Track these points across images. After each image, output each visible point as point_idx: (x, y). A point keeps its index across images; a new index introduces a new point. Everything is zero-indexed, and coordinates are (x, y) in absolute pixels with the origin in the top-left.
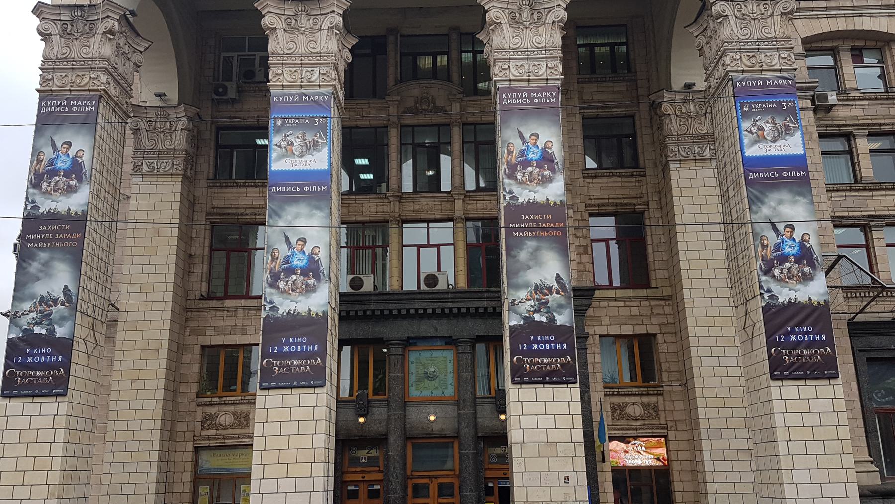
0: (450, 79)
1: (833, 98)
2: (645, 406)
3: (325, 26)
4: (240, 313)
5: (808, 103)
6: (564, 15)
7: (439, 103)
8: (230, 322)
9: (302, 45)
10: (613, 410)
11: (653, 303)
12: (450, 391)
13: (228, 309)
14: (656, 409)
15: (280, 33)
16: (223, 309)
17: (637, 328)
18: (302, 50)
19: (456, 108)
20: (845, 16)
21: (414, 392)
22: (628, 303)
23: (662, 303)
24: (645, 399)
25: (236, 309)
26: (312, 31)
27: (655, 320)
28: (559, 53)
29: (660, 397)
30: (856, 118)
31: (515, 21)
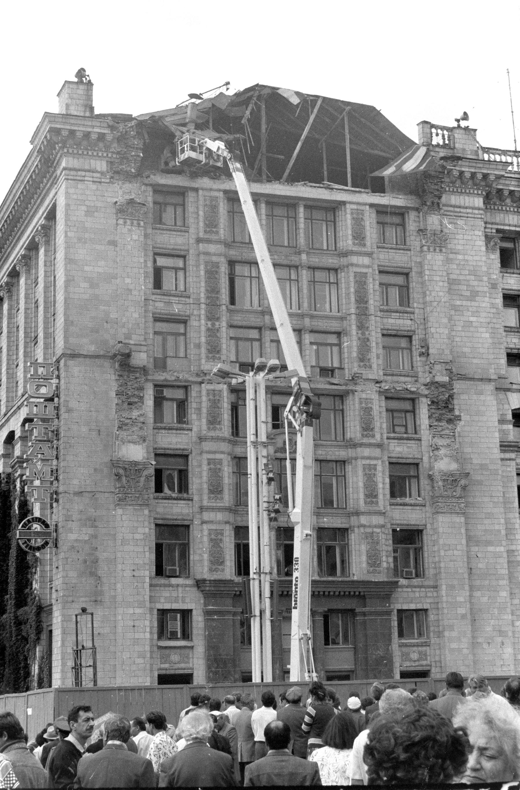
2: (420, 653)
4: (180, 589)
8: (174, 594)
10: (403, 655)
11: (427, 590)
13: (170, 585)
14: (426, 655)
16: (170, 585)
17: (418, 605)
22: (414, 589)
23: (432, 589)
24: (420, 649)
25: (178, 586)
27: (429, 600)
29: (428, 648)
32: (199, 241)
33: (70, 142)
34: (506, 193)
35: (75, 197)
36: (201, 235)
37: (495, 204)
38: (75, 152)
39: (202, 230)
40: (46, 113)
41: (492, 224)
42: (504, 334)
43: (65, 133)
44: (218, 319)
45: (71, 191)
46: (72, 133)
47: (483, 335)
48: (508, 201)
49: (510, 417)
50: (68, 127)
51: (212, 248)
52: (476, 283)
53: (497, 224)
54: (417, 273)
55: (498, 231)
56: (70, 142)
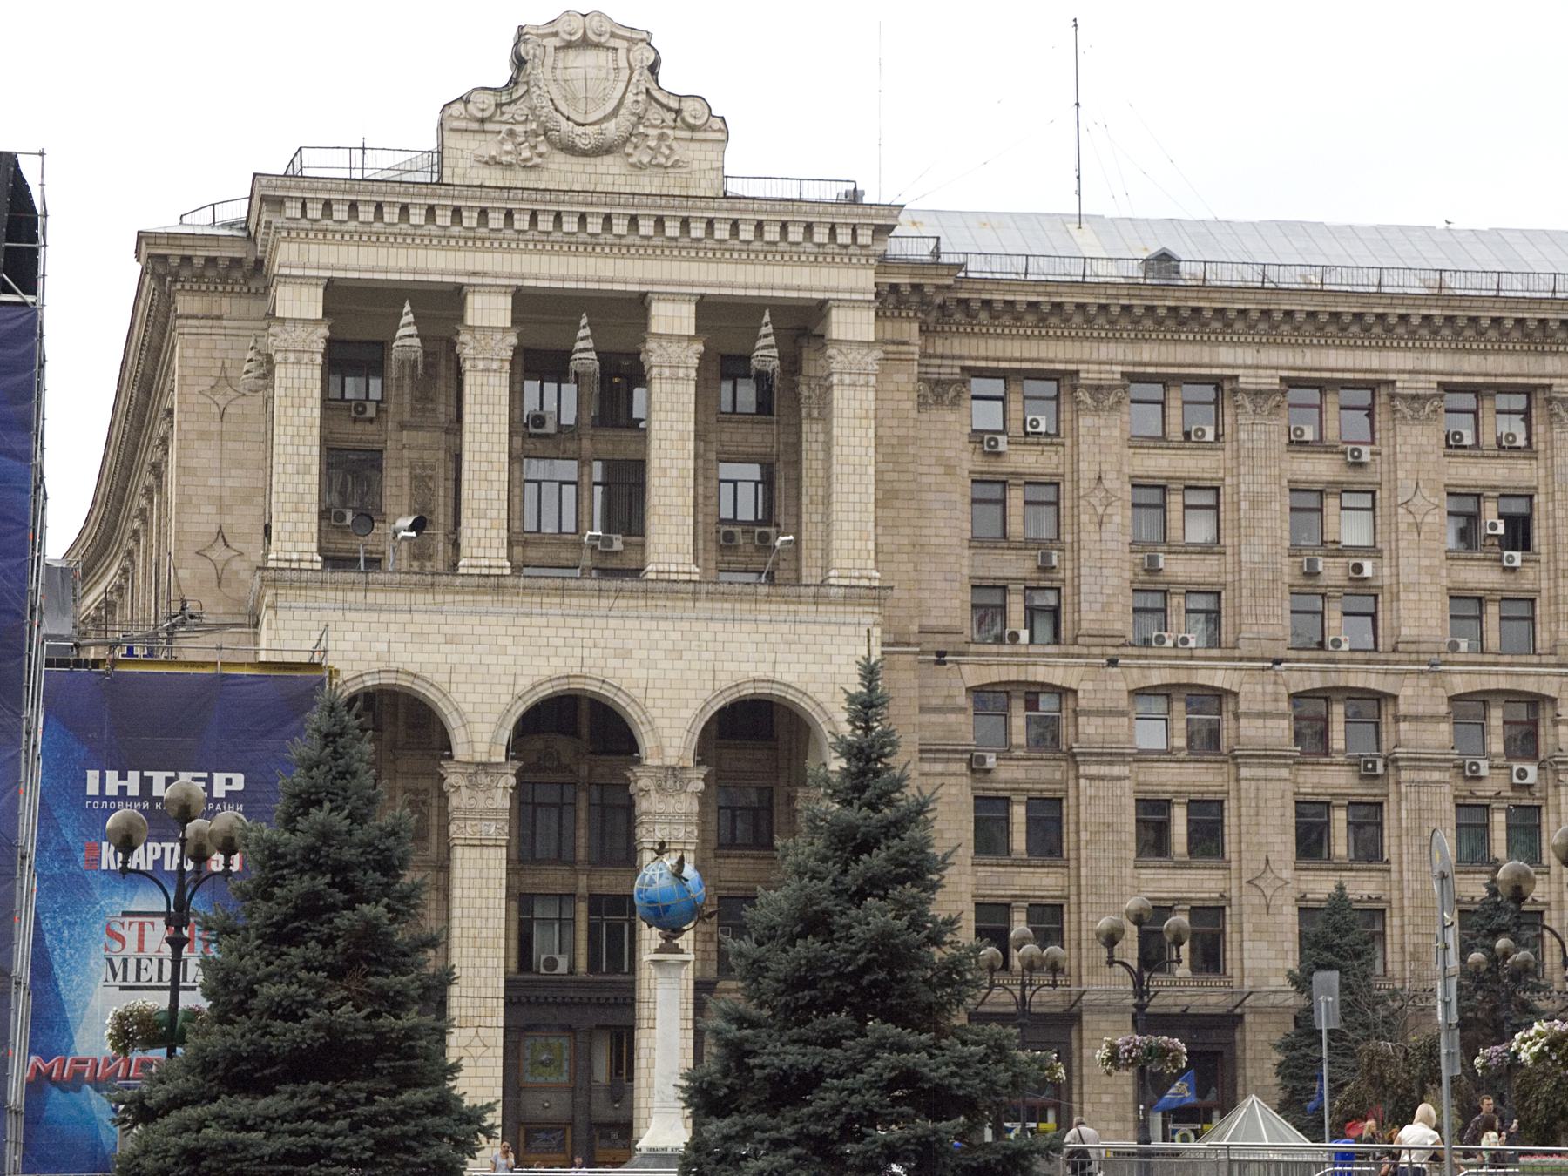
0: (575, 734)
1: (991, 761)
3: (501, 784)
5: (963, 767)
6: (701, 785)
7: (566, 760)
9: (481, 801)
12: (565, 1078)
15: (463, 790)
18: (481, 805)
19: (584, 770)
20: (1018, 664)
21: (529, 1079)
26: (489, 787)
28: (695, 819)
30: (1016, 781)
31: (661, 789)
32: (403, 426)
33: (185, 273)
34: (976, 306)
35: (194, 362)
36: (407, 417)
37: (958, 324)
38: (195, 287)
39: (407, 408)
40: (142, 236)
41: (953, 357)
42: (967, 552)
43: (174, 262)
44: (430, 558)
45: (189, 353)
46: (187, 260)
47: (903, 567)
48: (983, 316)
49: (962, 700)
50: (181, 252)
51: (421, 437)
52: (895, 476)
53: (961, 358)
54: (787, 463)
55: (963, 368)
56: (185, 273)
